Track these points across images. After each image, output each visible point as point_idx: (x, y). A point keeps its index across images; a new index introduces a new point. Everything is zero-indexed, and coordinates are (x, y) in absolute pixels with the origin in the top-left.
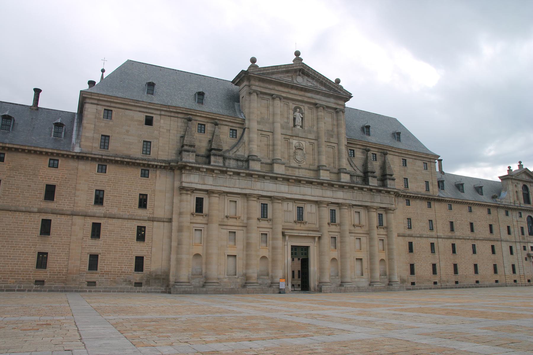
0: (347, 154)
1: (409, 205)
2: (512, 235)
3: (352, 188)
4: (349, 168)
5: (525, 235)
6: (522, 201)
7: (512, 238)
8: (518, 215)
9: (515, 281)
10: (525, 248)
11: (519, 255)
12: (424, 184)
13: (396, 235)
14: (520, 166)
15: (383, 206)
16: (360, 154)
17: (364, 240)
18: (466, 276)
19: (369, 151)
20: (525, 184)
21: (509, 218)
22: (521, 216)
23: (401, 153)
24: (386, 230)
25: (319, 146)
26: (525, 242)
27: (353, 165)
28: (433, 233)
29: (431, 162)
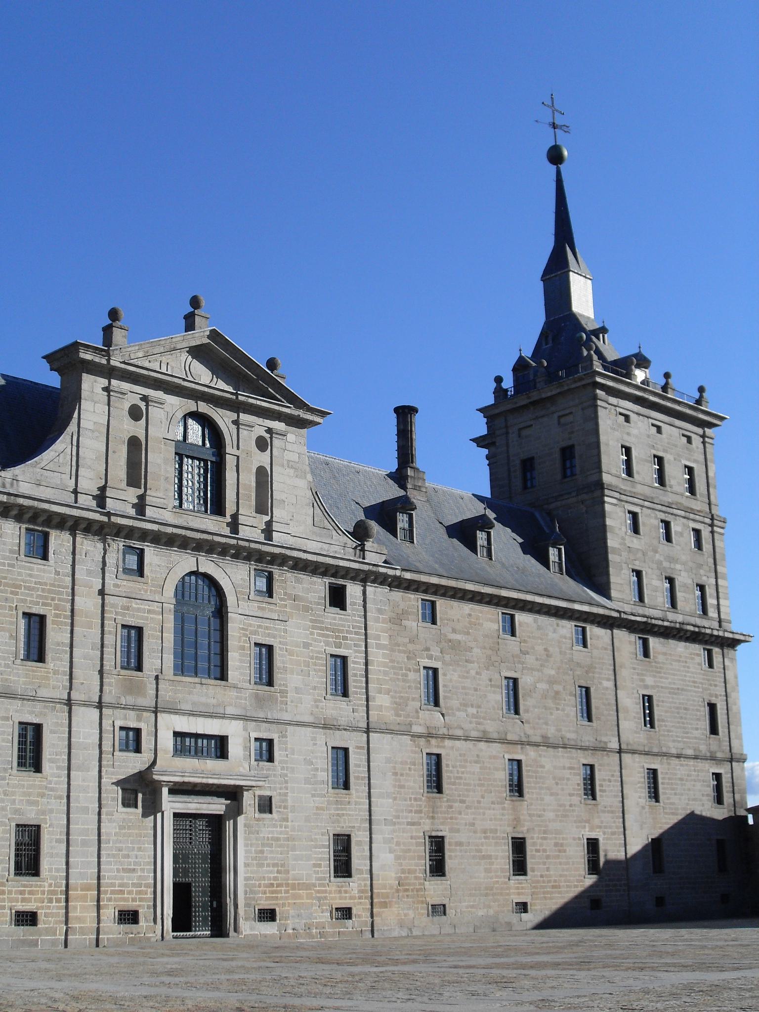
7: (50, 677)
11: (85, 780)
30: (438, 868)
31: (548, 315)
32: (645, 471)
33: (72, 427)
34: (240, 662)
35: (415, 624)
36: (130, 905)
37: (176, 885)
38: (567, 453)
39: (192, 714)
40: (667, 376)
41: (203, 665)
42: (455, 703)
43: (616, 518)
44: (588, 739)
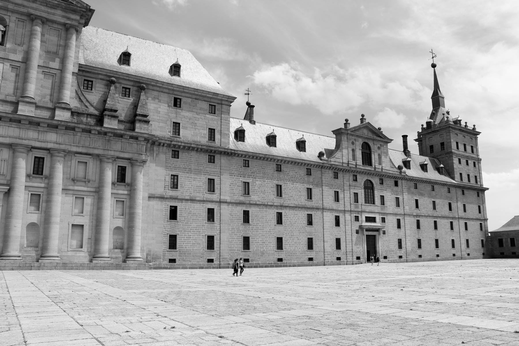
0: (75, 84)
1: (178, 158)
2: (341, 201)
3: (73, 129)
4: (74, 104)
5: (360, 203)
6: (360, 162)
7: (340, 206)
8: (351, 178)
9: (339, 259)
10: (357, 219)
11: (348, 228)
12: (206, 132)
13: (147, 195)
14: (362, 120)
15: (126, 155)
16: (103, 86)
17: (88, 201)
18: (263, 253)
19: (113, 82)
20: (366, 141)
21: (339, 181)
22: (356, 180)
23: (173, 90)
24: (129, 188)
25: (27, 70)
26: (358, 212)
27: (84, 100)
28: (214, 197)
29: (222, 104)
30: (420, 246)
31: (433, 108)
32: (461, 147)
33: (341, 148)
34: (378, 200)
35: (413, 189)
36: (358, 256)
37: (367, 251)
38: (442, 144)
39: (369, 212)
40: (466, 123)
41: (370, 202)
42: (422, 207)
43: (456, 161)
44: (451, 216)
